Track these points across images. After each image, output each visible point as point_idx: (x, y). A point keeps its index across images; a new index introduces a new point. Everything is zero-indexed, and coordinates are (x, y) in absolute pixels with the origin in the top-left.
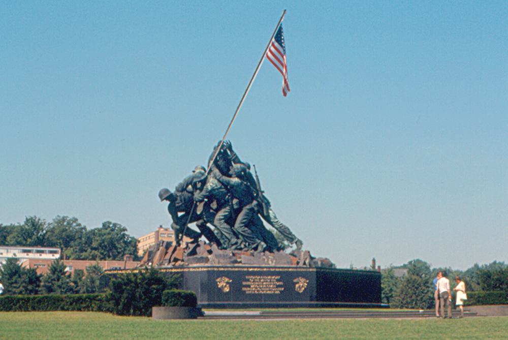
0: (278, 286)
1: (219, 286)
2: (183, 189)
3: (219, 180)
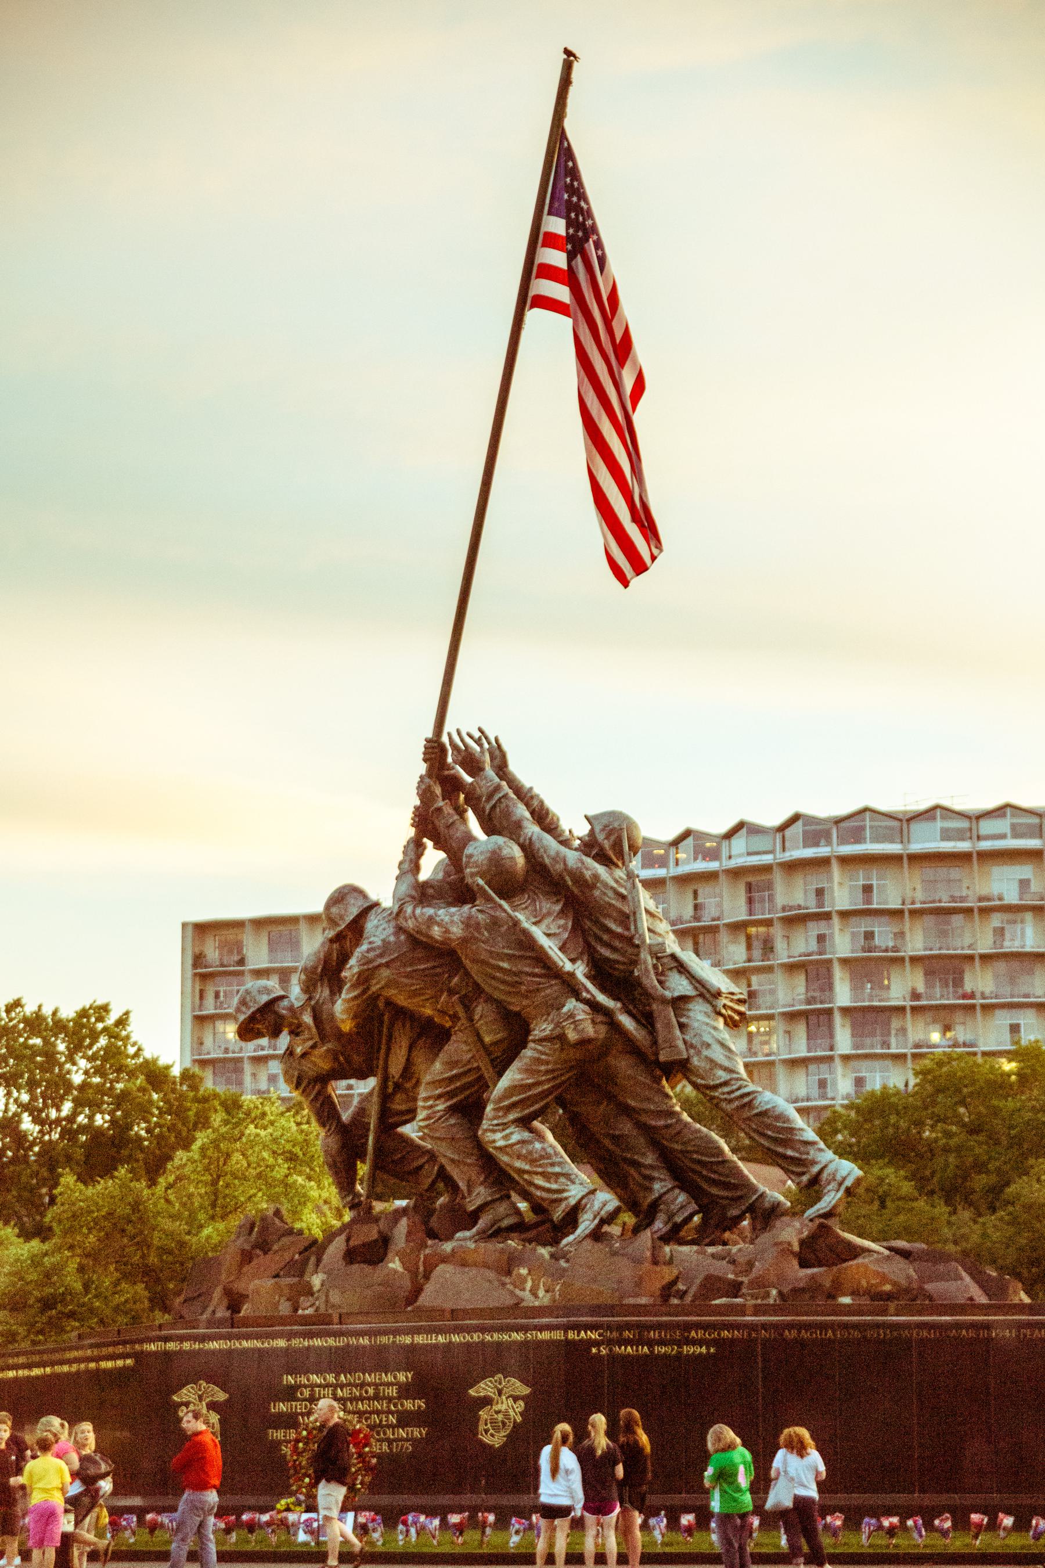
0: (405, 1420)
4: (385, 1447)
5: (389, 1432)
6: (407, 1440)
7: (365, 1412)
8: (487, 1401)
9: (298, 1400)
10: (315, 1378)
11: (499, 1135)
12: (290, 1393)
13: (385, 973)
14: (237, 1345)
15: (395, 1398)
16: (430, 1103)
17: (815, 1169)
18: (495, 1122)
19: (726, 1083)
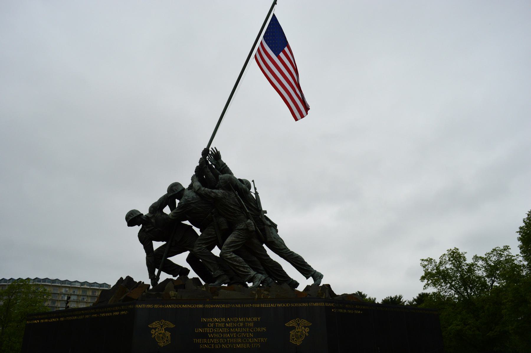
1: (153, 336)
2: (156, 208)
3: (197, 192)
4: (248, 345)
5: (250, 340)
6: (258, 343)
7: (239, 332)
8: (293, 328)
9: (208, 327)
12: (204, 325)
14: (180, 306)
17: (313, 273)
19: (285, 249)
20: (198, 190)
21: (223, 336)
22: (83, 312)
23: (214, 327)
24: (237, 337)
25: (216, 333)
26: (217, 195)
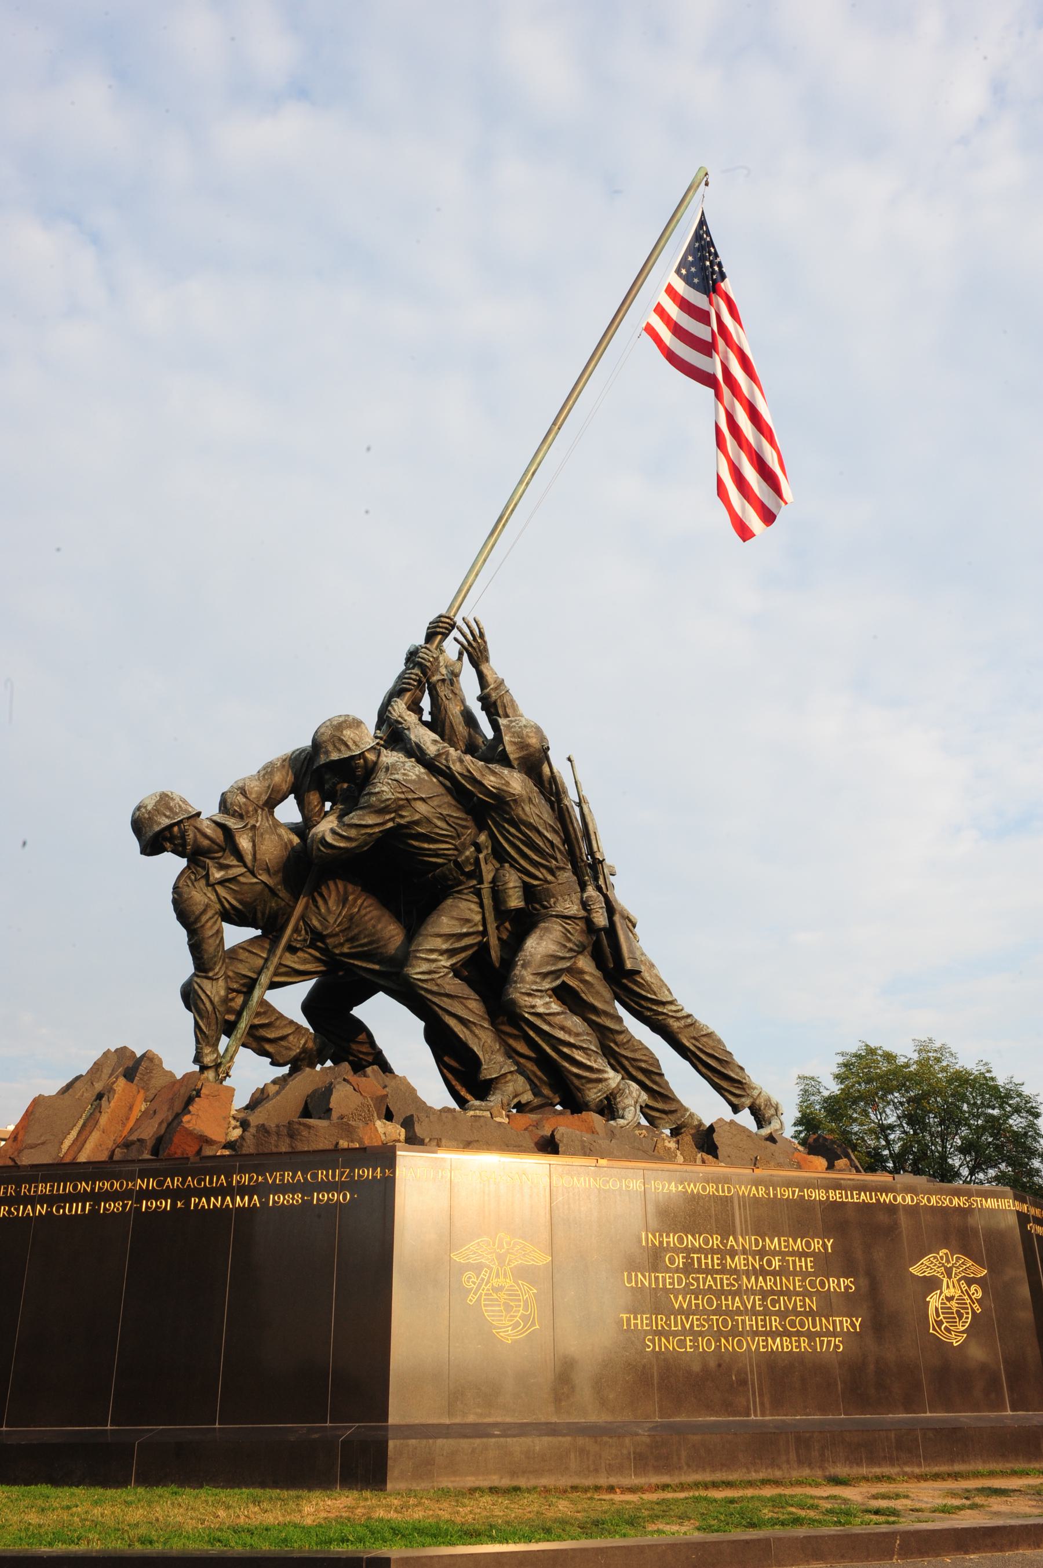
4: (804, 1344)
5: (808, 1323)
7: (772, 1292)
10: (689, 1240)
11: (538, 1002)
13: (421, 807)
15: (810, 1274)
16: (433, 956)
18: (535, 987)
19: (671, 1003)
20: (439, 755)
21: (719, 1306)
22: (82, 1186)
23: (688, 1269)
24: (766, 1312)
25: (697, 1293)
26: (508, 784)
